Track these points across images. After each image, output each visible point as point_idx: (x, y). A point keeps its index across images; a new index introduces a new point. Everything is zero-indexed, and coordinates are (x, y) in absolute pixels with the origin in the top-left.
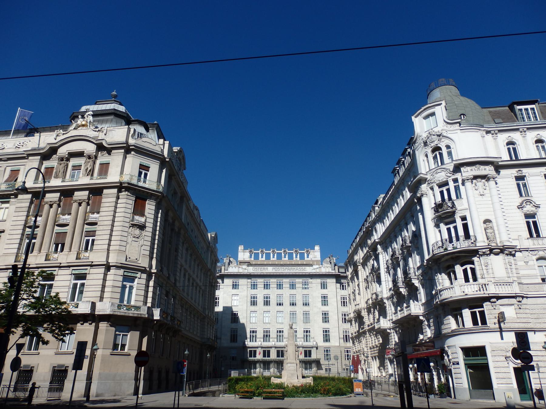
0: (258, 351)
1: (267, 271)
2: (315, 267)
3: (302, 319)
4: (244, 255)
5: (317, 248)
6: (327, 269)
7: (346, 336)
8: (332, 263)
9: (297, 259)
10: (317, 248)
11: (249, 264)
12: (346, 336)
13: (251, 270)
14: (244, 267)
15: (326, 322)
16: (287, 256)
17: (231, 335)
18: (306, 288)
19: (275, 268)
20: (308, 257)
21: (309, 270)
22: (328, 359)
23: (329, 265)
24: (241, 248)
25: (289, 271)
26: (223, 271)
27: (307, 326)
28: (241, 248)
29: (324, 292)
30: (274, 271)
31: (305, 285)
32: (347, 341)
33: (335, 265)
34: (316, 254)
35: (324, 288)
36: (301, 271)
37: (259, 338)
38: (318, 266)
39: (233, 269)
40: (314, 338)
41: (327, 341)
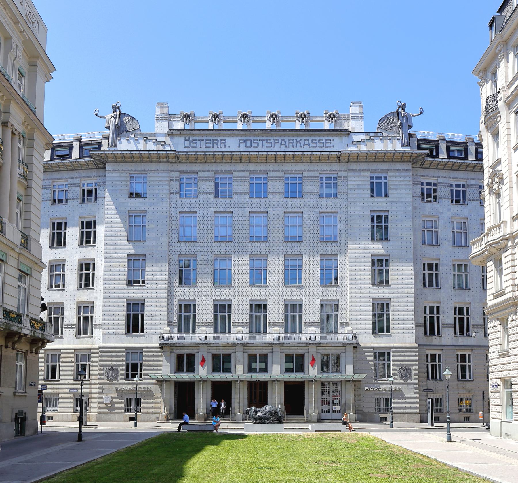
3: (317, 275)
7: (432, 319)
12: (432, 319)
17: (128, 316)
18: (328, 196)
19: (245, 142)
27: (331, 294)
29: (380, 204)
30: (243, 148)
31: (328, 185)
32: (432, 332)
35: (379, 195)
36: (317, 149)
41: (381, 331)
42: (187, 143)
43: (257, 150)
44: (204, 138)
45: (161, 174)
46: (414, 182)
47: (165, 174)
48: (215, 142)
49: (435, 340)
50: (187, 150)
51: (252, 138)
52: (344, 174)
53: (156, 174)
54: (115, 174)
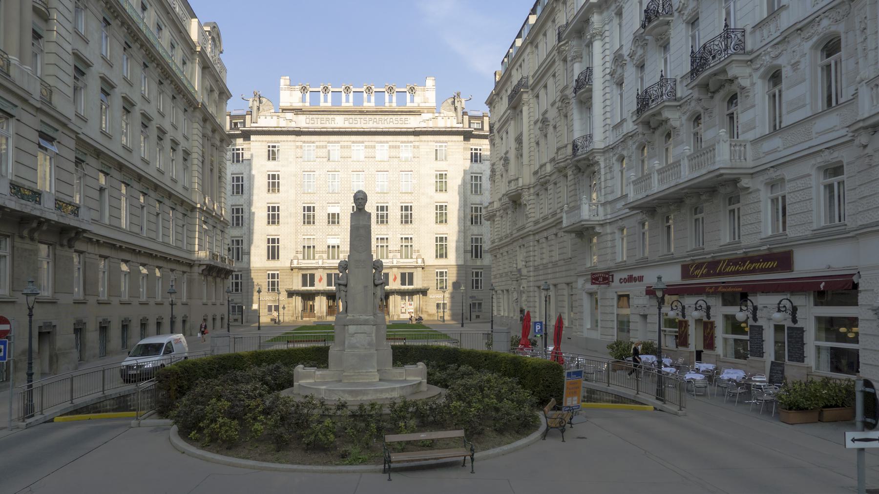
0: (318, 274)
1: (333, 125)
2: (425, 116)
4: (290, 97)
5: (430, 82)
6: (448, 120)
8: (459, 109)
9: (391, 102)
10: (430, 82)
11: (298, 111)
12: (476, 247)
13: (302, 122)
14: (290, 115)
15: (441, 222)
16: (373, 98)
20: (412, 101)
21: (413, 122)
22: (442, 288)
23: (453, 114)
24: (284, 81)
25: (375, 125)
26: (248, 124)
28: (284, 81)
32: (476, 256)
33: (464, 113)
34: (427, 95)
37: (320, 252)
38: (430, 116)
39: (266, 121)
40: (418, 251)
41: (441, 256)
42: (308, 121)
43: (356, 126)
44: (320, 116)
45: (289, 143)
46: (465, 149)
47: (293, 143)
48: (328, 120)
49: (479, 262)
50: (307, 126)
51: (353, 117)
52: (417, 144)
53: (286, 143)
54: (257, 143)
